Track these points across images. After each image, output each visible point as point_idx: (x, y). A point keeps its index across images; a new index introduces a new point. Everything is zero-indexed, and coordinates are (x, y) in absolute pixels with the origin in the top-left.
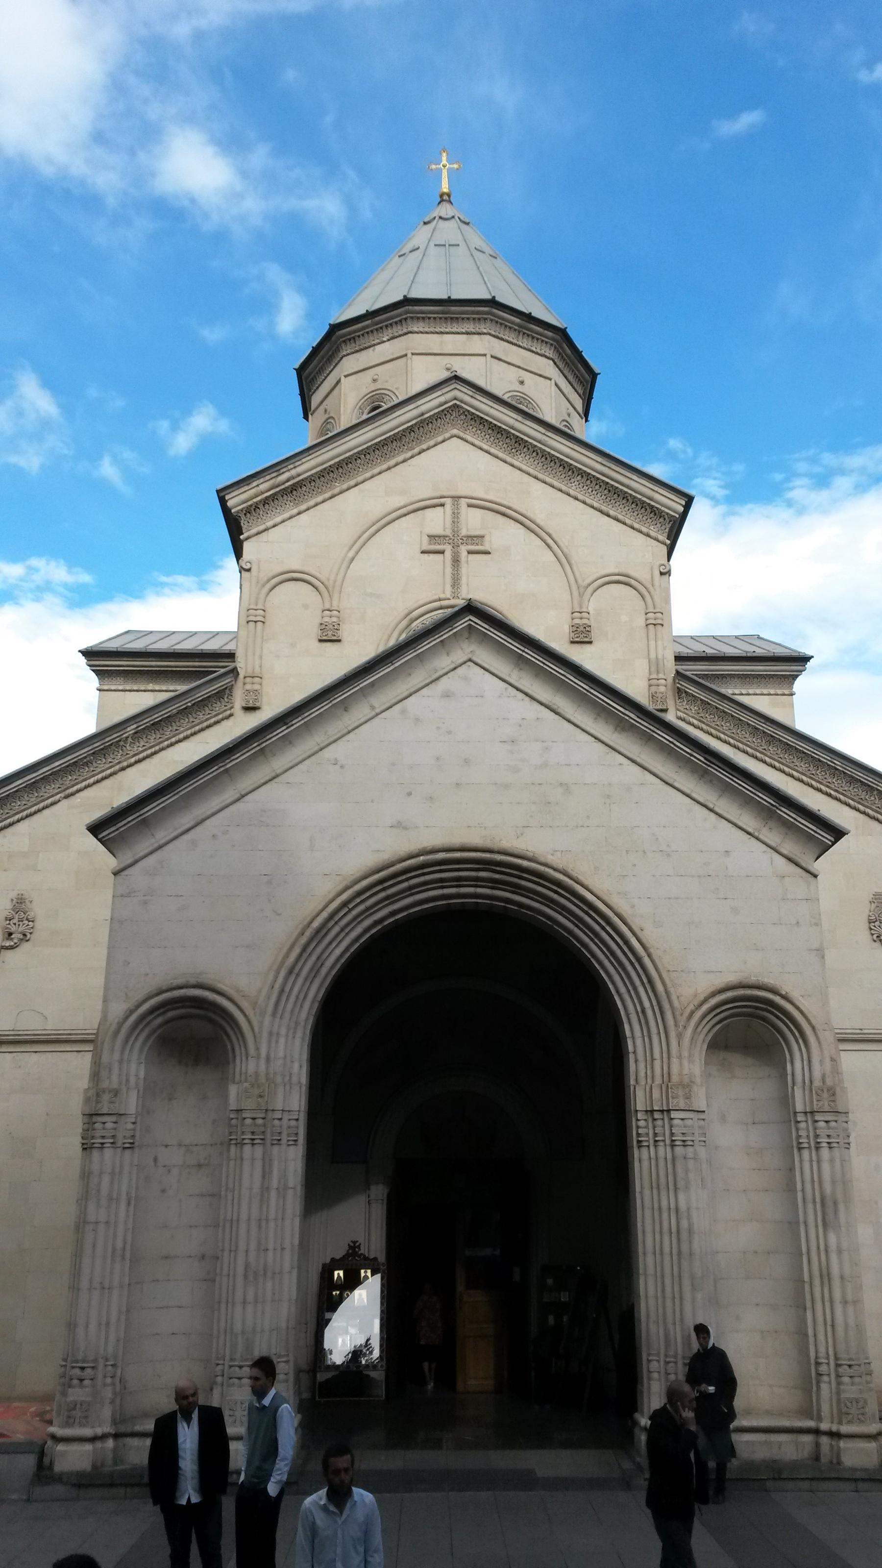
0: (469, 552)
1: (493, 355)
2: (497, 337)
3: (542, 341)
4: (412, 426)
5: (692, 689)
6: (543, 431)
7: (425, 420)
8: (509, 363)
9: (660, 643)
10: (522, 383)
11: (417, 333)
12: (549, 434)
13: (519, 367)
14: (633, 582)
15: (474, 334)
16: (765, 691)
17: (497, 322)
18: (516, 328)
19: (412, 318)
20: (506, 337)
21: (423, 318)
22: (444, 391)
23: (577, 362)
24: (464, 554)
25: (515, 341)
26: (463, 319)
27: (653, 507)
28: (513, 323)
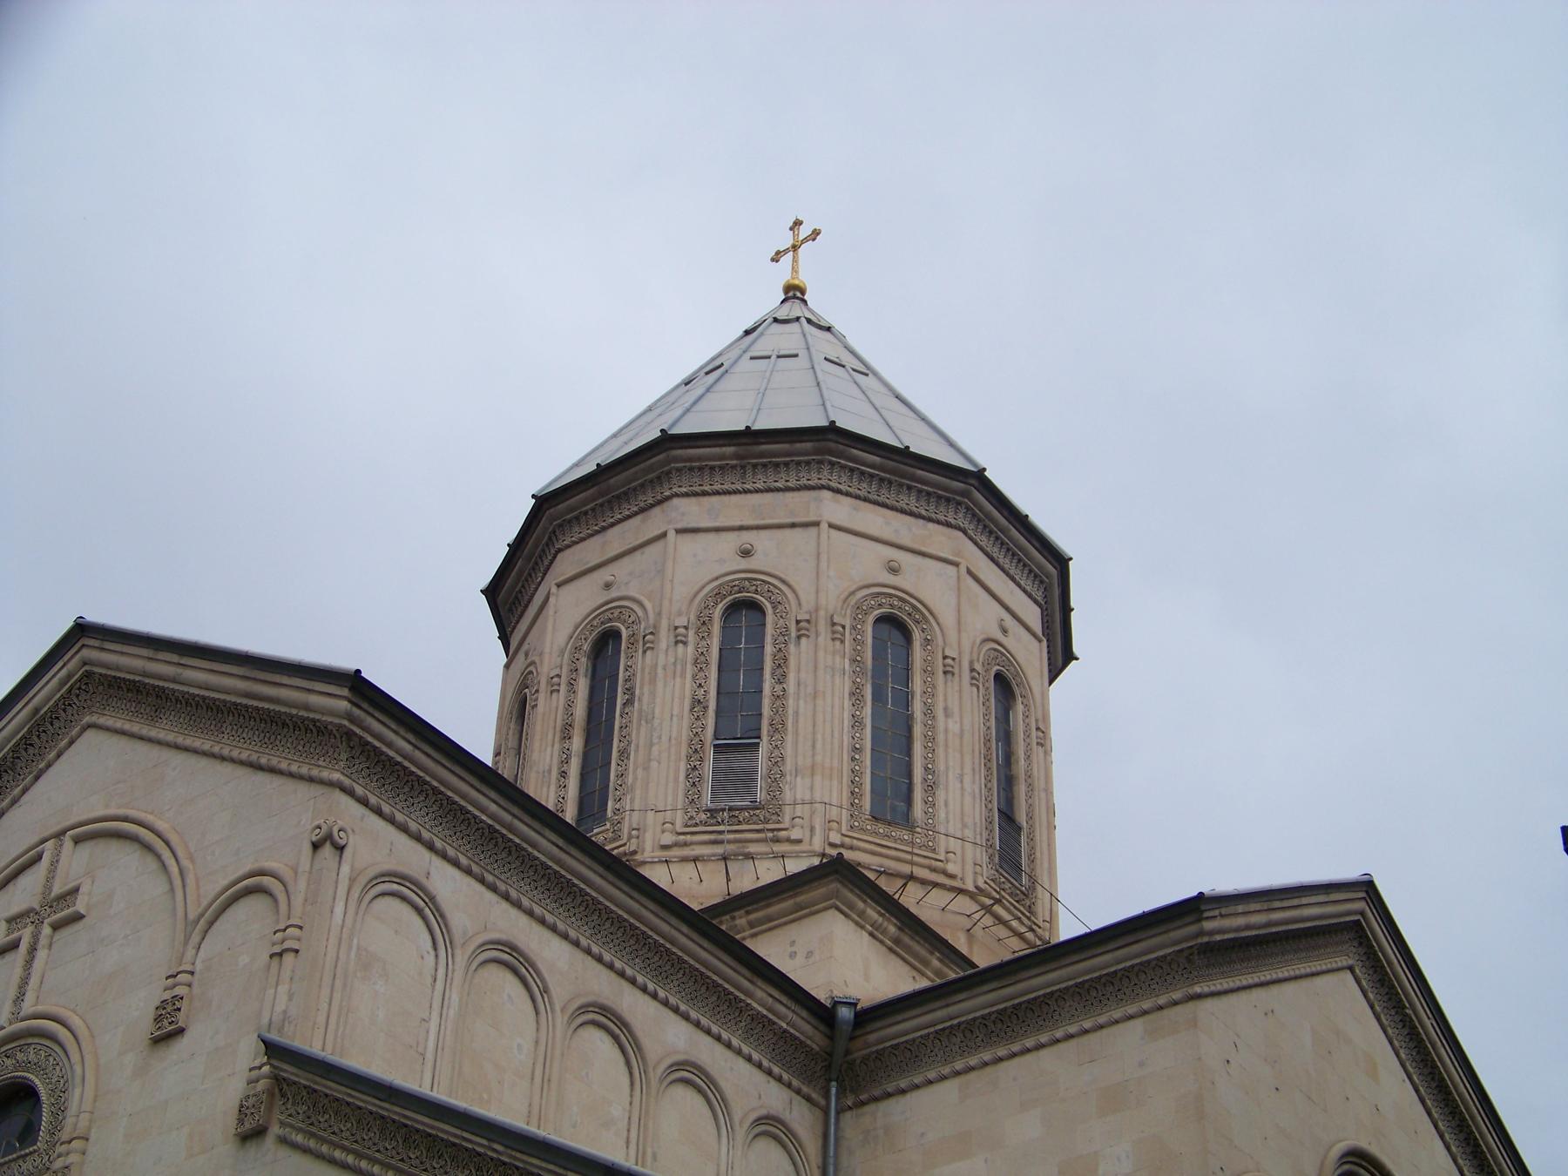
0: (56, 927)
1: (679, 526)
2: (696, 494)
3: (799, 463)
4: (24, 737)
5: (289, 1071)
6: (175, 658)
7: (43, 718)
8: (717, 530)
9: (283, 989)
10: (746, 553)
11: (568, 547)
12: (184, 661)
13: (741, 528)
14: (266, 880)
15: (652, 506)
16: (1132, 1009)
17: (691, 469)
18: (734, 462)
19: (560, 525)
20: (717, 487)
21: (577, 518)
22: (66, 658)
23: (920, 472)
24: (47, 930)
25: (739, 486)
26: (635, 489)
27: (314, 721)
28: (722, 457)
